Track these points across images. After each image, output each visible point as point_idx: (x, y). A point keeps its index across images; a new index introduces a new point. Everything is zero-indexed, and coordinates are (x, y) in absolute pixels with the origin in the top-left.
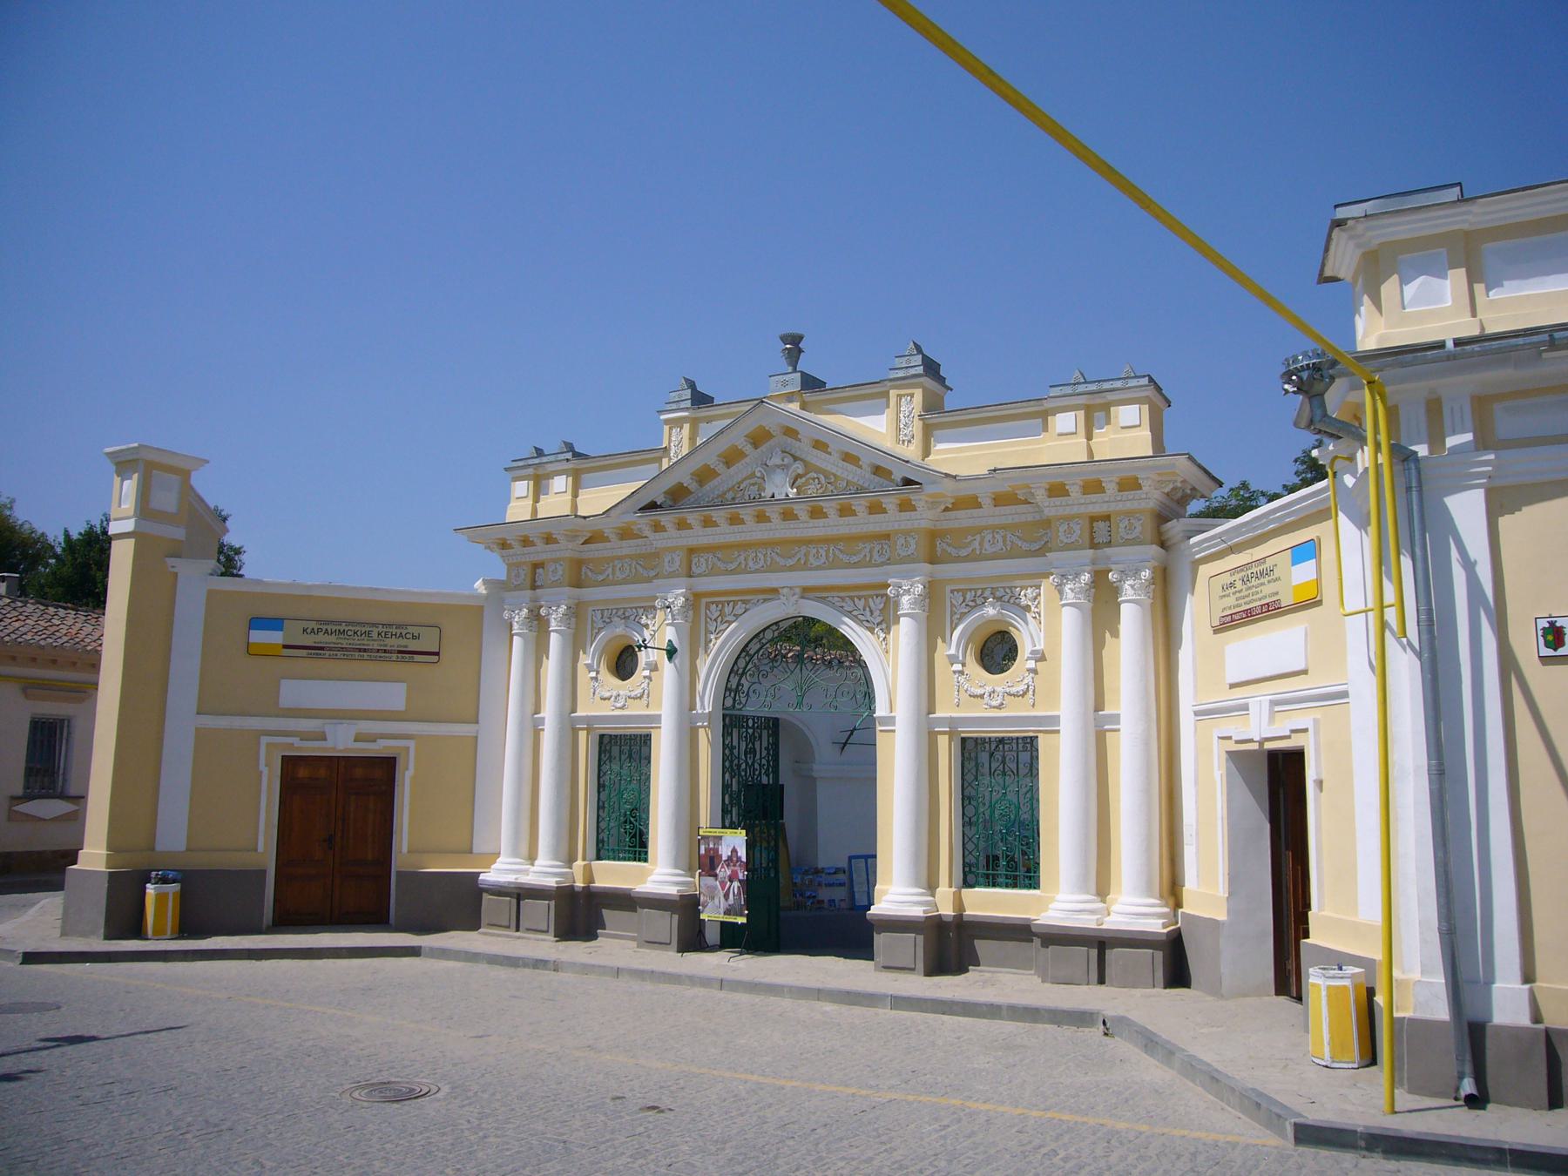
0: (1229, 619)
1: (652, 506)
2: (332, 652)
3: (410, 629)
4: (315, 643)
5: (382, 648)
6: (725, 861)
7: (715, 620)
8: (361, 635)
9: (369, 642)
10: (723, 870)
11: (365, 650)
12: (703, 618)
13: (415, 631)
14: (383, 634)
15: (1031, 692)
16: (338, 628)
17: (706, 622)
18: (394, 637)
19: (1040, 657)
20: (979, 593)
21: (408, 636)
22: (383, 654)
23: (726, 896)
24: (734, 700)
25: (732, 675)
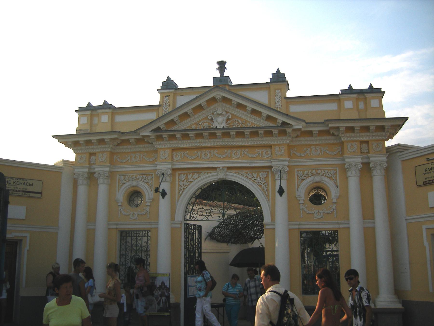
0: (431, 181)
1: (158, 129)
3: (29, 181)
5: (15, 189)
6: (158, 288)
7: (183, 181)
10: (157, 292)
12: (177, 179)
13: (31, 182)
14: (16, 183)
15: (335, 213)
17: (179, 181)
18: (21, 184)
20: (310, 171)
21: (27, 184)
22: (15, 192)
23: (159, 304)
24: (190, 217)
25: (188, 205)
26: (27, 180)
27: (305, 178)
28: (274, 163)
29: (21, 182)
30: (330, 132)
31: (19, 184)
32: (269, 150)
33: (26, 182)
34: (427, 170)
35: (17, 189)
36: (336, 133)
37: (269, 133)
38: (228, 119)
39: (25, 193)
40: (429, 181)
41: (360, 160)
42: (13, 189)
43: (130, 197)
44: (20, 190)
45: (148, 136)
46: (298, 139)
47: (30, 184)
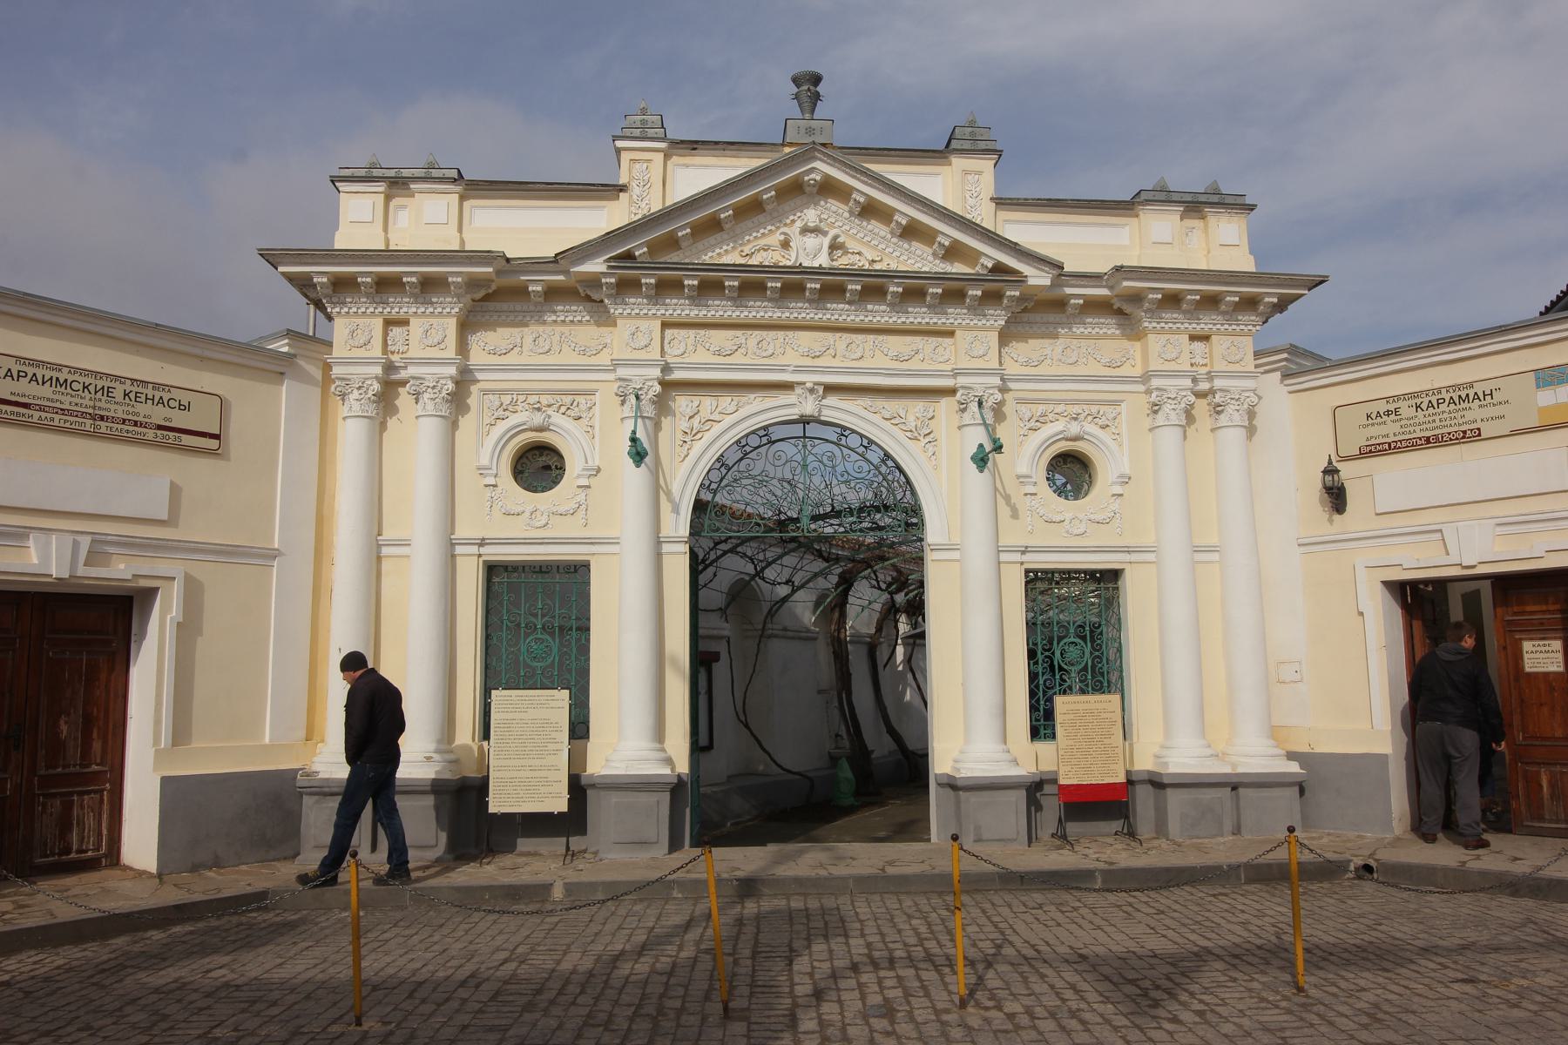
1: (629, 256)
2: (44, 415)
3: (176, 394)
5: (130, 417)
8: (96, 392)
9: (108, 406)
11: (102, 418)
13: (185, 398)
14: (132, 396)
16: (55, 374)
18: (150, 402)
19: (1125, 480)
21: (172, 403)
22: (131, 428)
27: (1037, 424)
28: (962, 381)
30: (1112, 305)
31: (143, 400)
32: (947, 341)
33: (166, 397)
34: (1374, 416)
35: (135, 418)
36: (1127, 308)
37: (954, 293)
38: (835, 246)
39: (165, 433)
40: (1379, 444)
41: (1188, 383)
42: (120, 415)
43: (517, 462)
44: (147, 420)
45: (594, 281)
46: (1026, 317)
47: (180, 405)
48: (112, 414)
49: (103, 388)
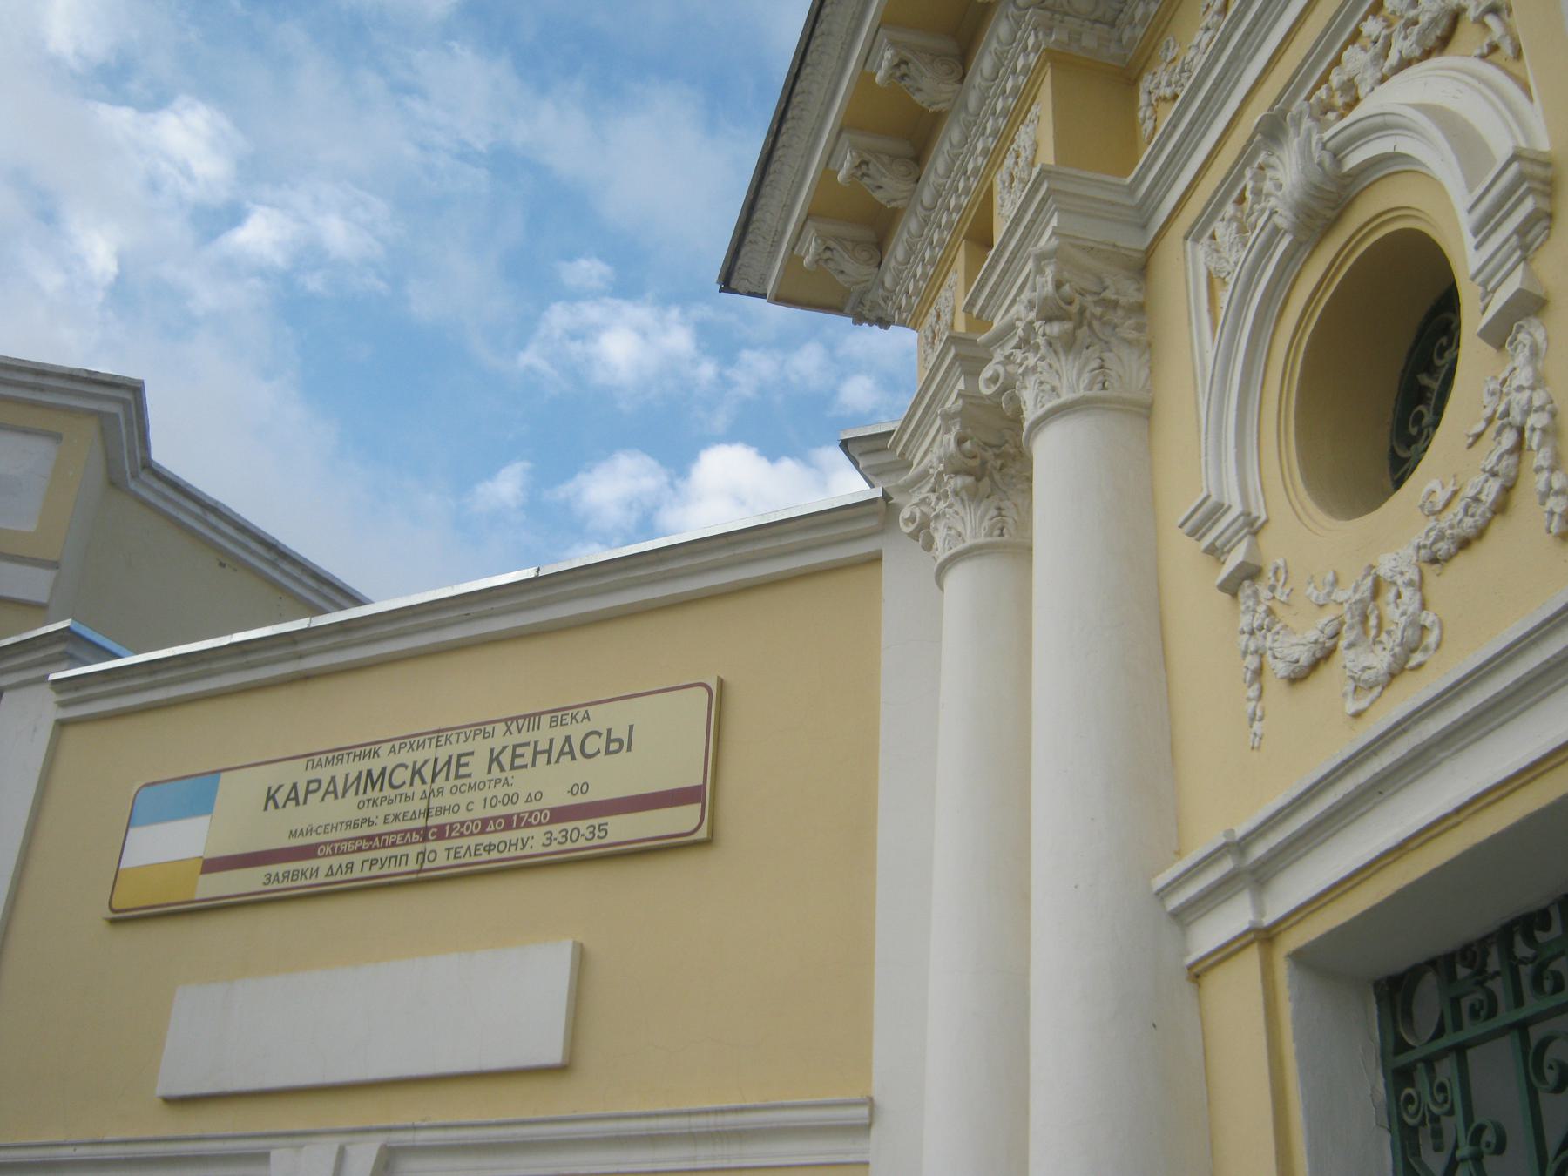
2: (335, 861)
3: (601, 717)
4: (292, 834)
5: (500, 810)
8: (434, 776)
11: (441, 833)
14: (506, 759)
16: (364, 765)
21: (593, 744)
26: (591, 709)
29: (543, 746)
31: (528, 759)
33: (576, 731)
35: (510, 809)
39: (569, 826)
42: (480, 812)
47: (609, 741)
48: (463, 815)
49: (449, 762)
